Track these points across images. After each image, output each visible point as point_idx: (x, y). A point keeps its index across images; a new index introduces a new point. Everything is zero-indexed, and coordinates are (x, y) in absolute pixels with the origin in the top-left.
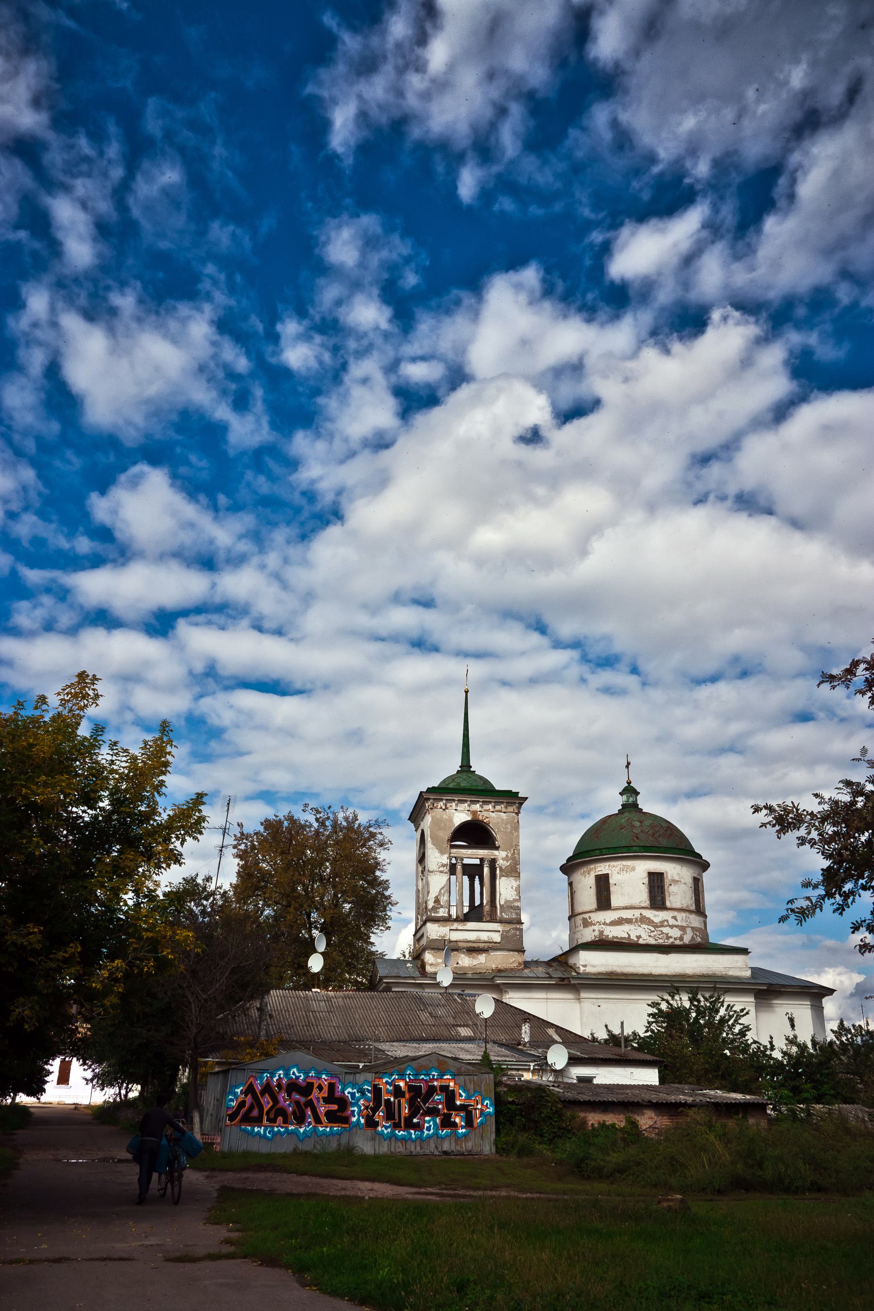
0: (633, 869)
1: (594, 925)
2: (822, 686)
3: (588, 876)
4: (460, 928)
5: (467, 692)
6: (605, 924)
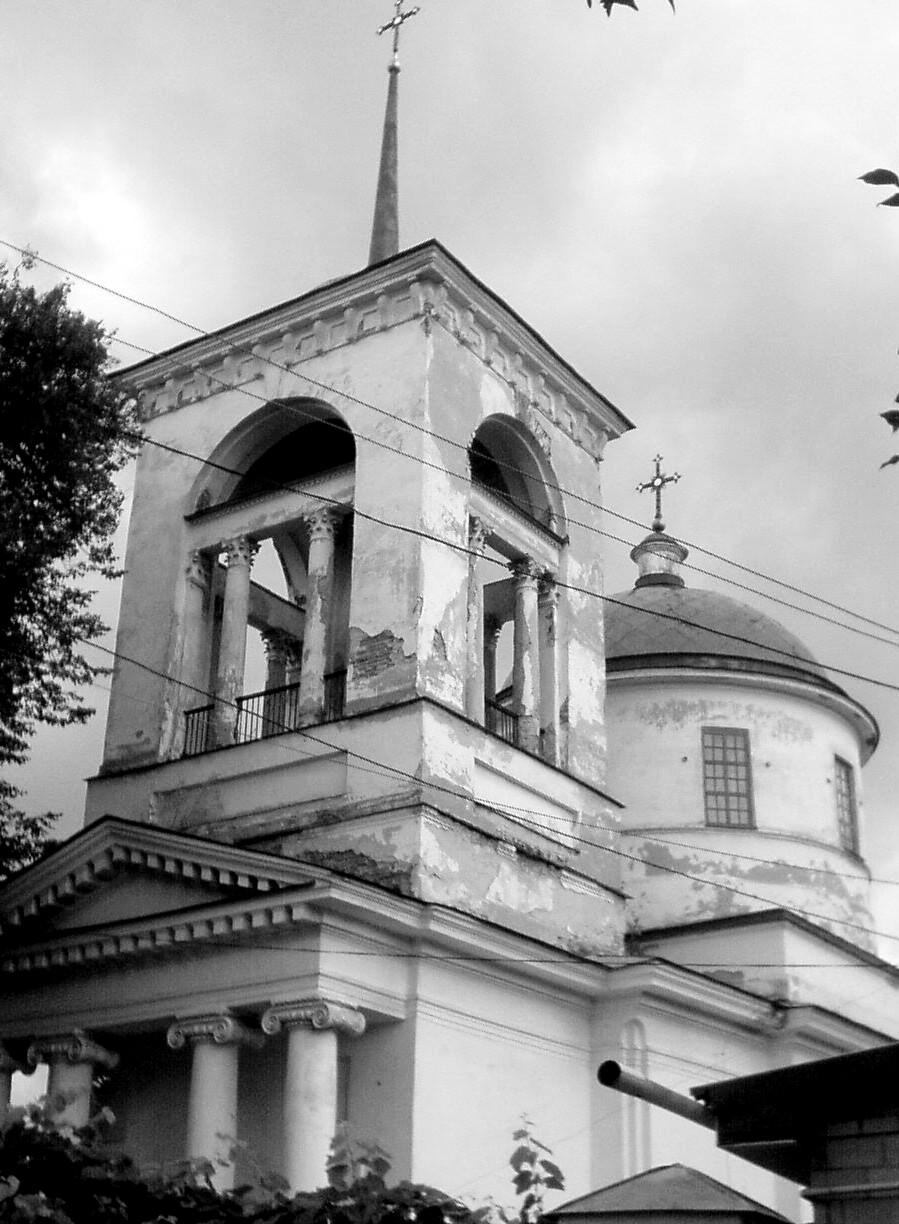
0: (808, 735)
1: (696, 869)
2: (106, 626)
3: (671, 724)
4: (498, 765)
5: (394, 70)
6: (733, 871)
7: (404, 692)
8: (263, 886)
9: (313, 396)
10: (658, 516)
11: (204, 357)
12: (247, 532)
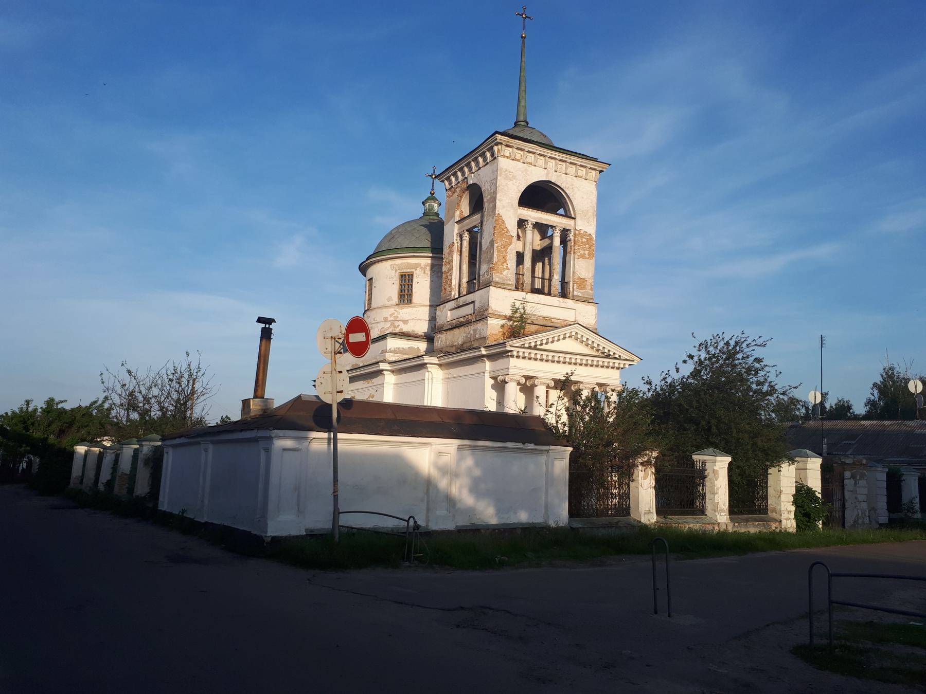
7: (592, 299)
8: (617, 356)
9: (562, 187)
10: (433, 189)
11: (530, 150)
12: (535, 221)
